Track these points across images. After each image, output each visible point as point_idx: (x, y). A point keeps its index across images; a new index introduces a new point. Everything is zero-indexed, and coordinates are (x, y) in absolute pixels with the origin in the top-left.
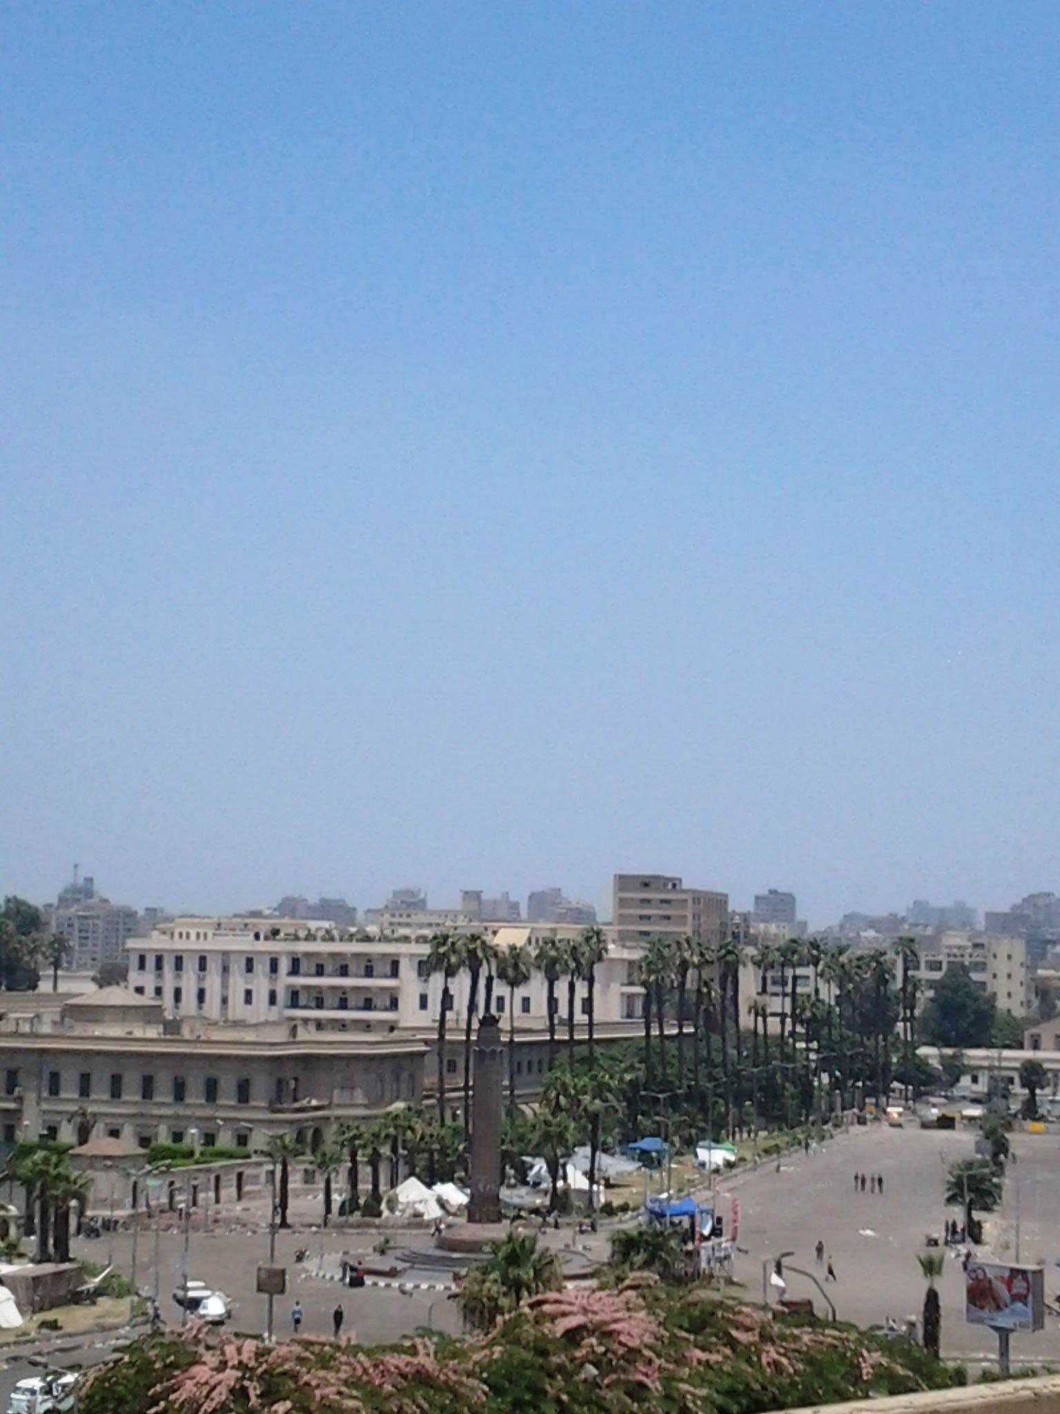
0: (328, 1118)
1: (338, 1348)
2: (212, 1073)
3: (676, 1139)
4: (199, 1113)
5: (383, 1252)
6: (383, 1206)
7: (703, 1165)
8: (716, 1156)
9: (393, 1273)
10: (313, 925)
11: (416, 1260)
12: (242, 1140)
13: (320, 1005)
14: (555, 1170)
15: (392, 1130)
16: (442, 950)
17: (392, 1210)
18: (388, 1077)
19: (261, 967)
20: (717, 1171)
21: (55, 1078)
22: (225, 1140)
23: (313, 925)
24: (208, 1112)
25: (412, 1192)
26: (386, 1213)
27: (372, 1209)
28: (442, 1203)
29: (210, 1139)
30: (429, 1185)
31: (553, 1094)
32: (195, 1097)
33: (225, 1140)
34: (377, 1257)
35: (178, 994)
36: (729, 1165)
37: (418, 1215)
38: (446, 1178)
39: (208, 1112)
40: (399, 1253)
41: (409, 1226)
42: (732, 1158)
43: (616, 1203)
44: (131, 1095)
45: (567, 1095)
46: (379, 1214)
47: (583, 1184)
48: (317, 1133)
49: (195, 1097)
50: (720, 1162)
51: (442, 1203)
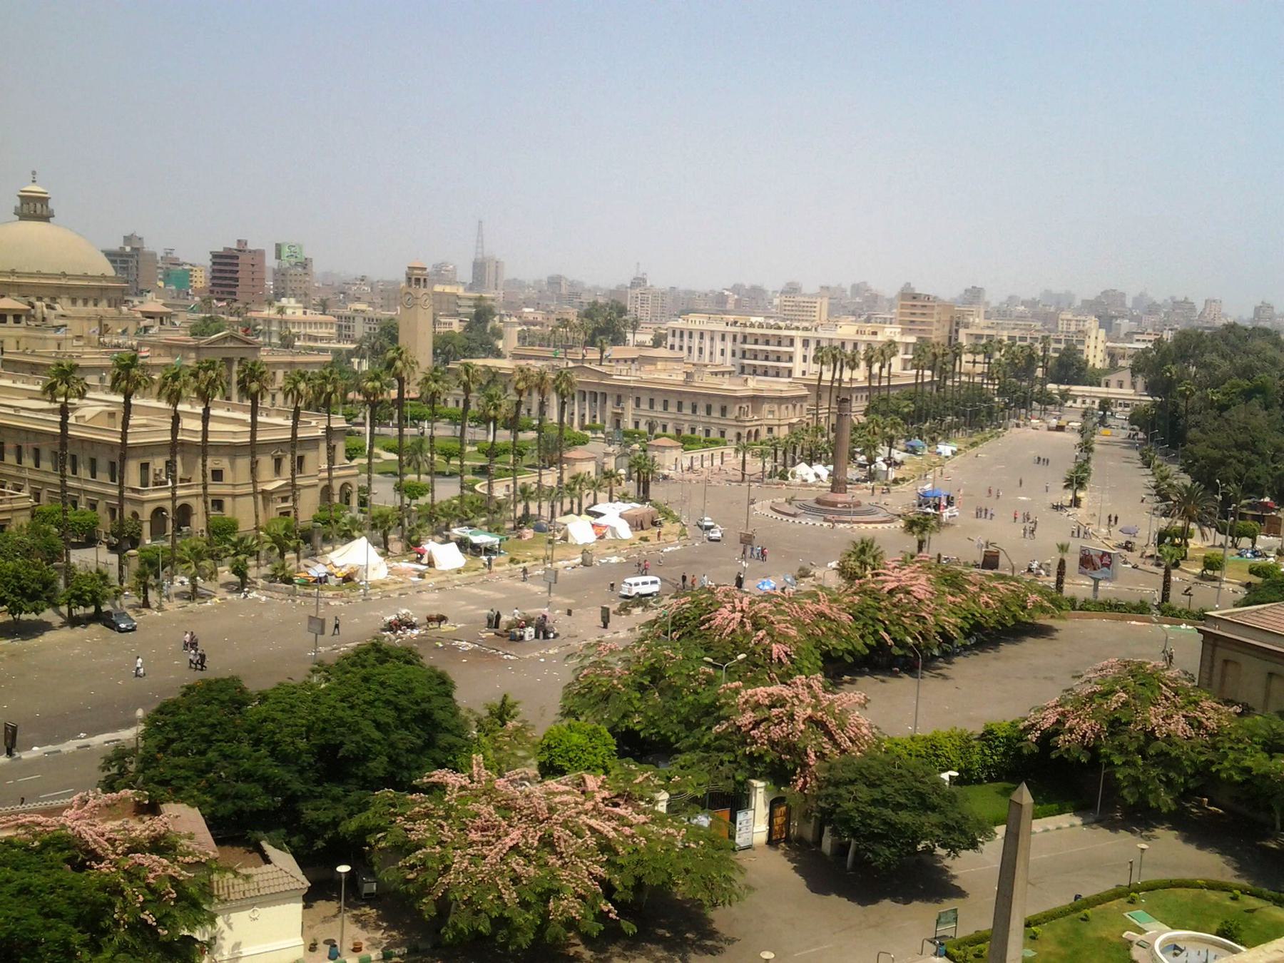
0: (761, 425)
1: (784, 599)
2: (710, 403)
3: (928, 439)
4: (703, 420)
5: (790, 504)
6: (789, 475)
7: (940, 453)
8: (945, 449)
9: (794, 515)
10: (753, 319)
11: (807, 509)
12: (723, 434)
13: (755, 358)
14: (871, 461)
15: (794, 440)
16: (820, 354)
17: (793, 478)
18: (790, 406)
19: (729, 339)
20: (947, 457)
21: (638, 399)
22: (714, 434)
23: (753, 319)
24: (707, 420)
25: (803, 469)
26: (790, 479)
27: (783, 477)
28: (817, 476)
29: (708, 432)
30: (810, 465)
31: (871, 426)
32: (701, 412)
33: (714, 434)
34: (787, 505)
35: (690, 349)
36: (954, 453)
37: (806, 481)
38: (818, 460)
39: (707, 420)
40: (798, 503)
41: (801, 485)
42: (955, 449)
43: (900, 476)
44: (673, 409)
45: (878, 426)
46: (787, 479)
47: (884, 467)
48: (757, 431)
49: (701, 412)
50: (949, 454)
51: (817, 476)
